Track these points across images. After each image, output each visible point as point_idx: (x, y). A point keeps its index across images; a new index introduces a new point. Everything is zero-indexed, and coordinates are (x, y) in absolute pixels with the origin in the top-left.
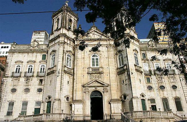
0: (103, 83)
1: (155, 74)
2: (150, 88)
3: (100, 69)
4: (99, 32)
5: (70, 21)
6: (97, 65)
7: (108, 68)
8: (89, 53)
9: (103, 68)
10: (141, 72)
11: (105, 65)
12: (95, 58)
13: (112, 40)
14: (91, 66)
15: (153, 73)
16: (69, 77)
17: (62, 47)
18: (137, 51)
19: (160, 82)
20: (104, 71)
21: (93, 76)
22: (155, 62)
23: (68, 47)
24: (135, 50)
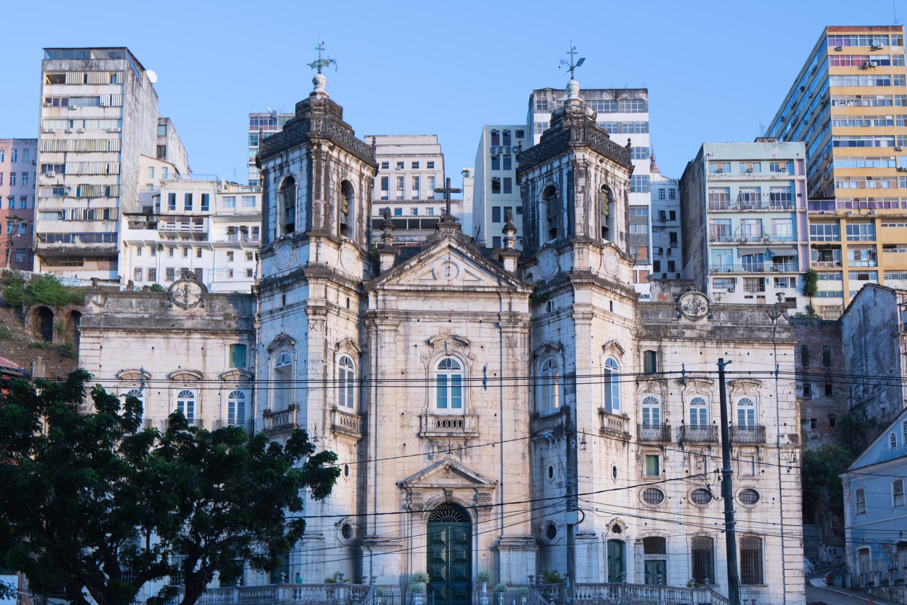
0: (474, 476)
1: (681, 444)
2: (654, 496)
3: (467, 420)
4: (469, 255)
5: (346, 187)
6: (457, 404)
7: (498, 417)
8: (426, 349)
9: (478, 417)
10: (625, 439)
11: (485, 403)
12: (449, 374)
13: (523, 293)
14: (434, 408)
15: (674, 436)
16: (347, 448)
17: (318, 327)
18: (620, 348)
19: (699, 472)
20: (484, 429)
21: (439, 447)
22: (693, 389)
23: (342, 322)
24: (616, 346)
